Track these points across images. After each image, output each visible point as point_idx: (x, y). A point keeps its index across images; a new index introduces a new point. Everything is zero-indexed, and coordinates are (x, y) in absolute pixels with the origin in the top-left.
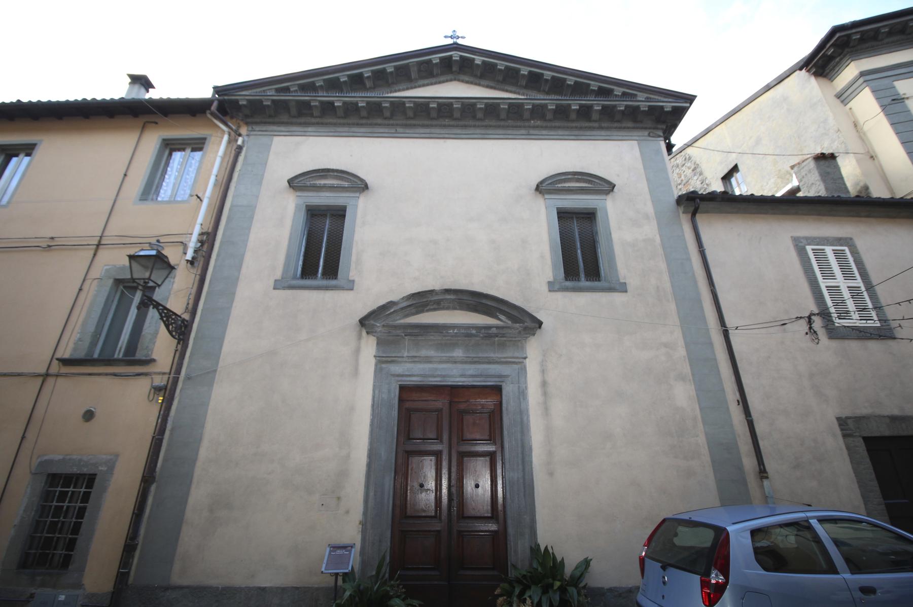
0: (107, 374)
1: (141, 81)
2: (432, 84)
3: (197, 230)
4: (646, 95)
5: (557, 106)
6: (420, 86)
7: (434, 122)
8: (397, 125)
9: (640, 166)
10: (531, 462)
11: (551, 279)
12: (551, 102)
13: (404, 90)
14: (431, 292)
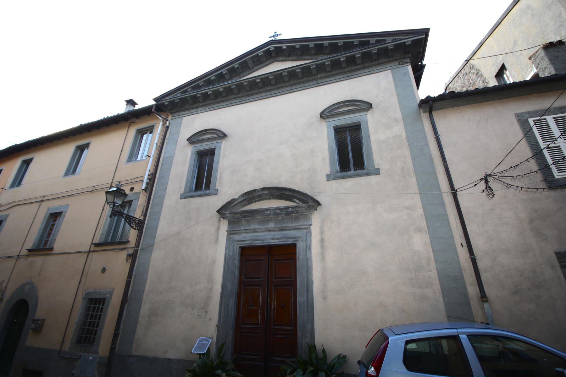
0: (111, 250)
1: (131, 102)
2: (262, 68)
3: (147, 173)
4: (392, 38)
5: (331, 61)
6: (255, 71)
7: (262, 90)
8: (242, 96)
9: (392, 86)
10: (312, 291)
11: (329, 173)
12: (325, 59)
13: (247, 75)
14: (255, 191)
